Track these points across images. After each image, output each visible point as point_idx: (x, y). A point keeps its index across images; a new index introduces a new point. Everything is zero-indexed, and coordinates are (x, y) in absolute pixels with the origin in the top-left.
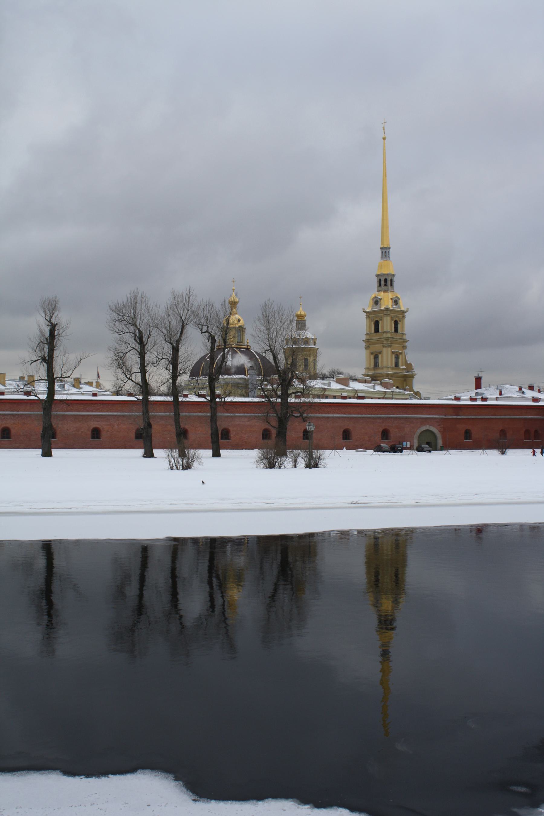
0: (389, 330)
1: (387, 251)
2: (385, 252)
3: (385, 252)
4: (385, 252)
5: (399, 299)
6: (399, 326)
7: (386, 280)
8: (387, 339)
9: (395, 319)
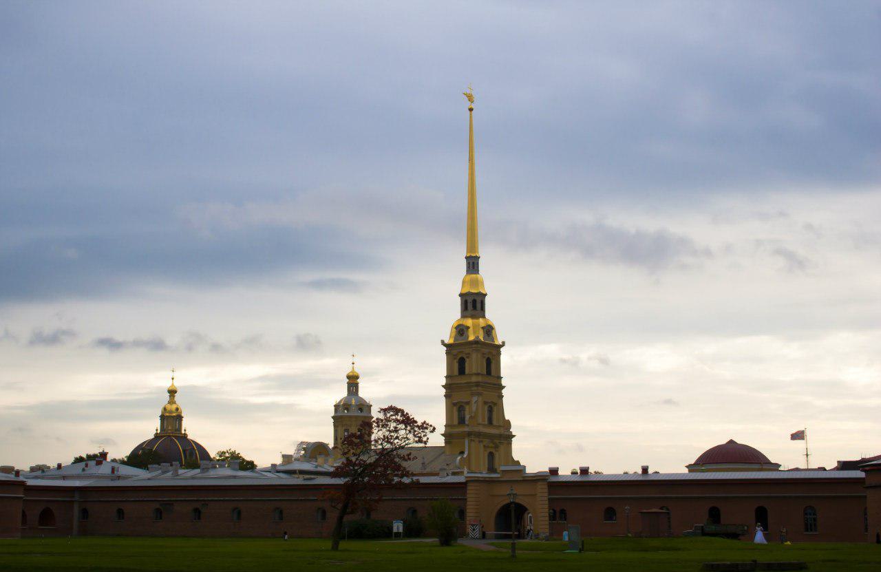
1: (476, 262)
2: (473, 263)
6: (493, 366)
7: (474, 302)
8: (477, 384)
9: (487, 356)
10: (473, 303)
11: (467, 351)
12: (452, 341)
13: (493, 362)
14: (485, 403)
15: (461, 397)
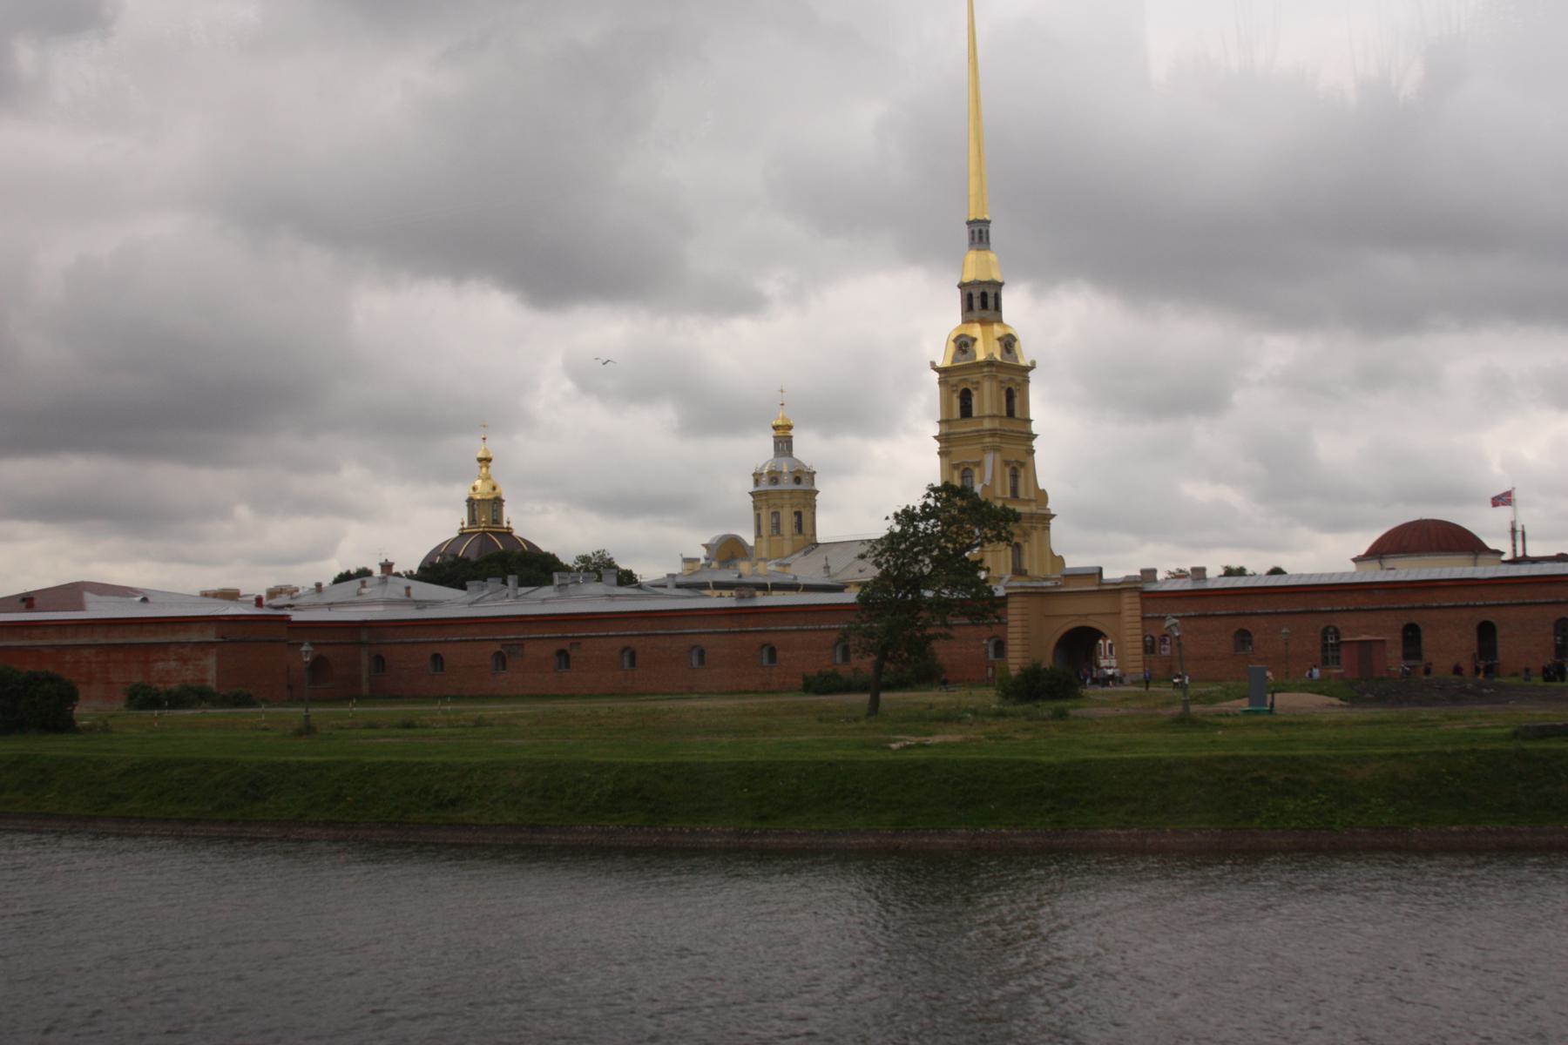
6: (1017, 401)
7: (984, 296)
8: (993, 433)
12: (948, 363)
13: (1017, 394)
14: (1007, 463)
15: (964, 453)
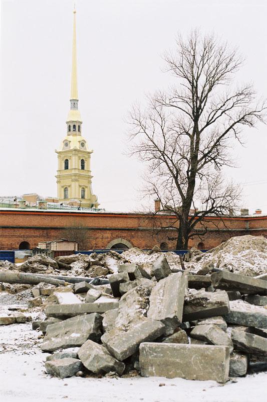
0: (77, 167)
1: (76, 102)
3: (74, 103)
4: (74, 103)
5: (85, 142)
6: (85, 164)
7: (74, 126)
10: (74, 128)
11: (71, 155)
